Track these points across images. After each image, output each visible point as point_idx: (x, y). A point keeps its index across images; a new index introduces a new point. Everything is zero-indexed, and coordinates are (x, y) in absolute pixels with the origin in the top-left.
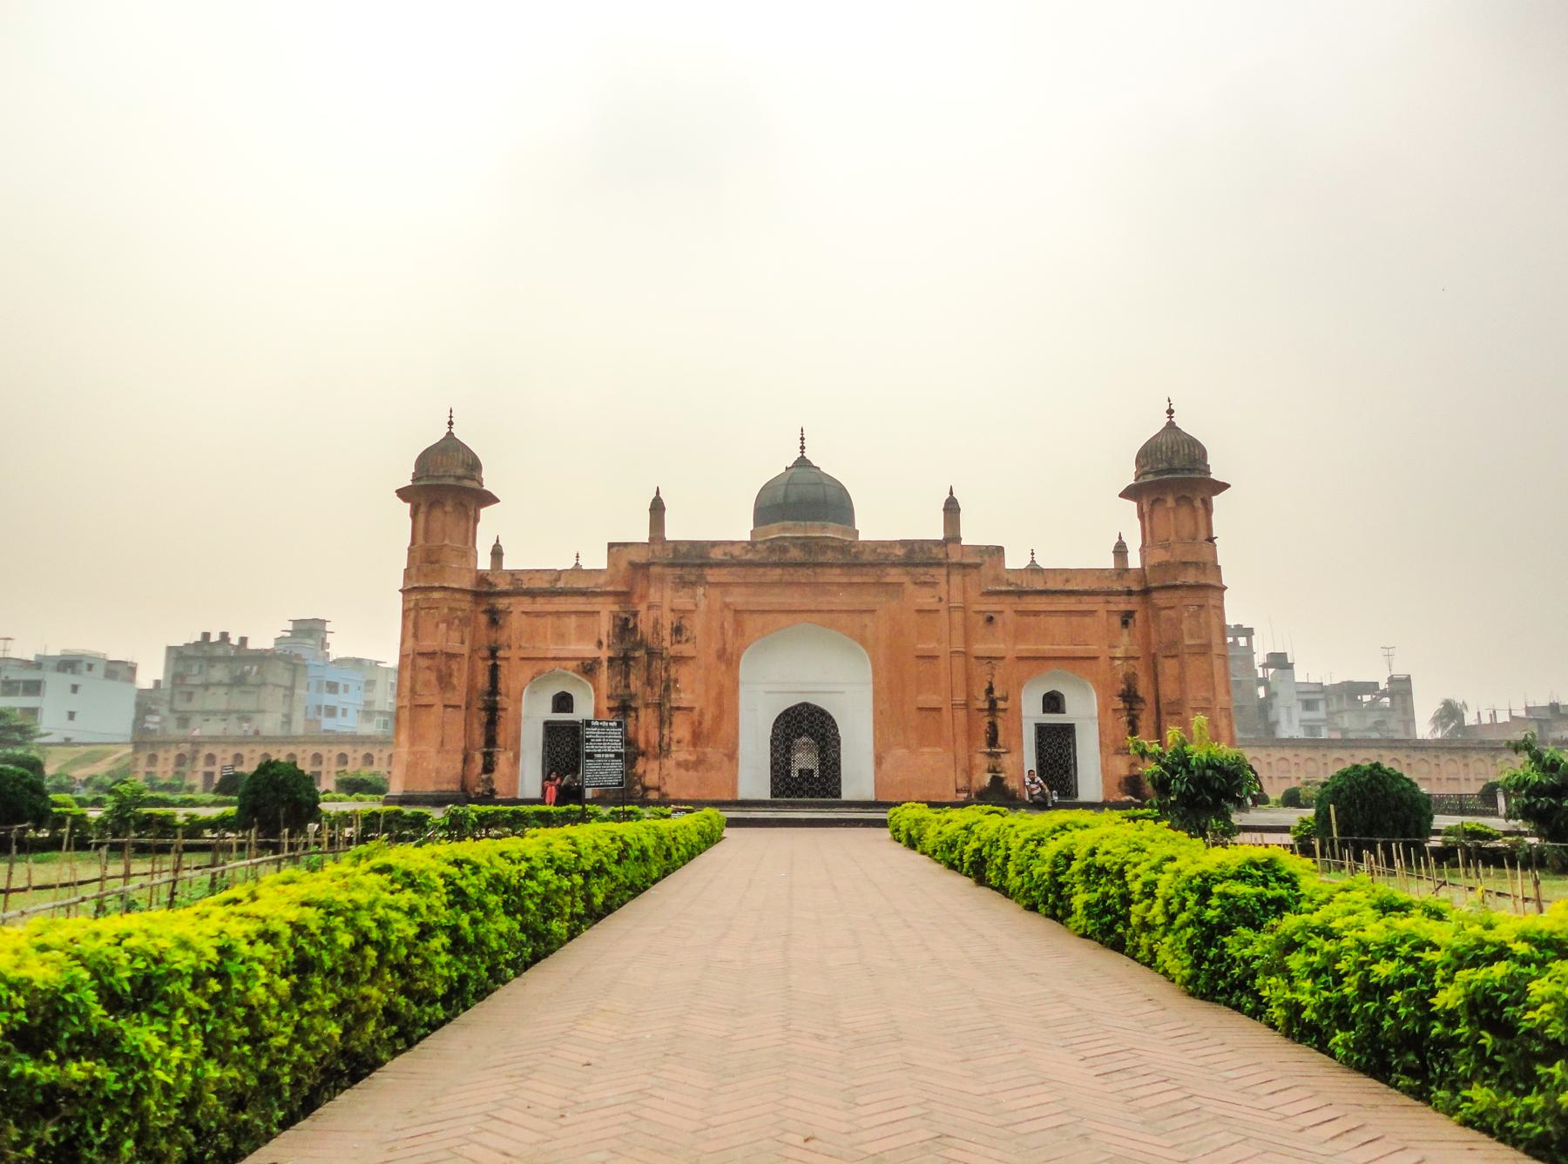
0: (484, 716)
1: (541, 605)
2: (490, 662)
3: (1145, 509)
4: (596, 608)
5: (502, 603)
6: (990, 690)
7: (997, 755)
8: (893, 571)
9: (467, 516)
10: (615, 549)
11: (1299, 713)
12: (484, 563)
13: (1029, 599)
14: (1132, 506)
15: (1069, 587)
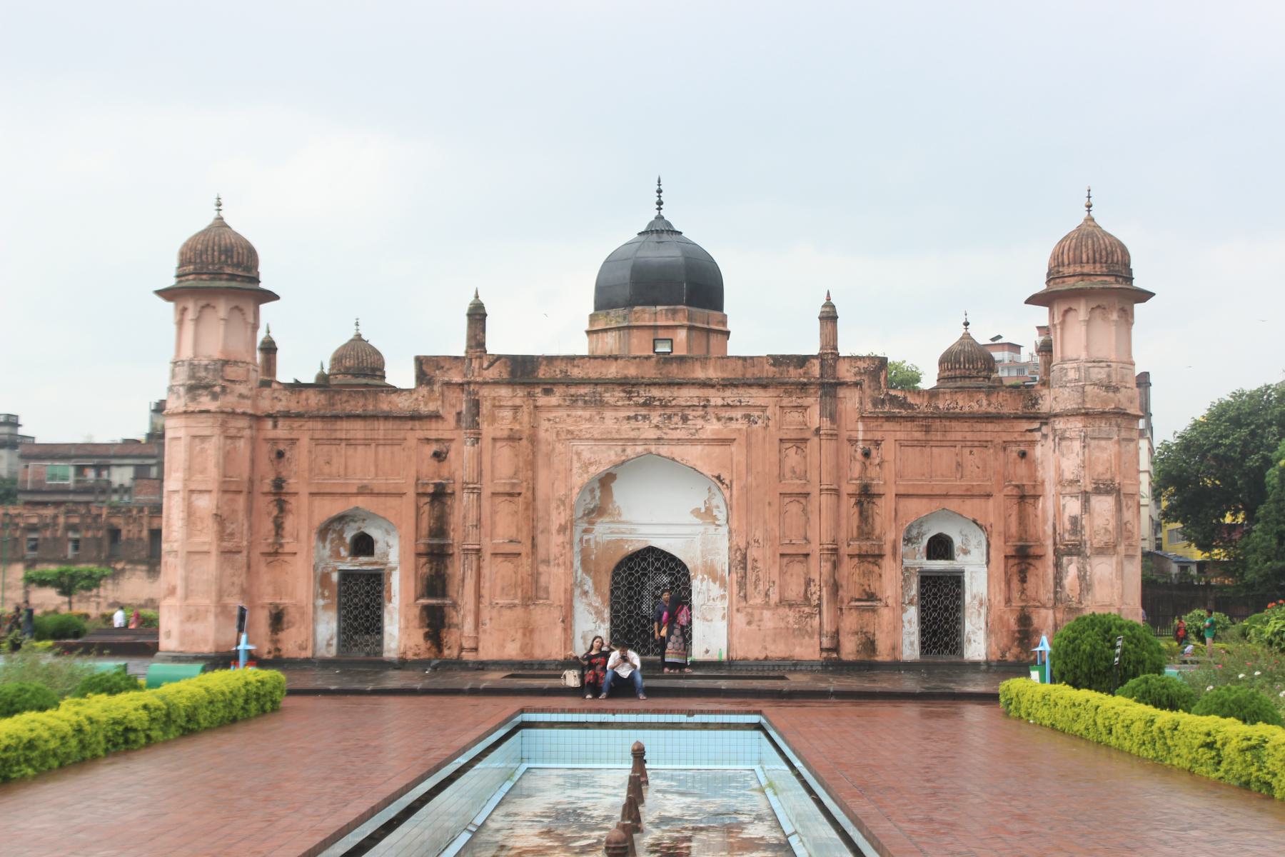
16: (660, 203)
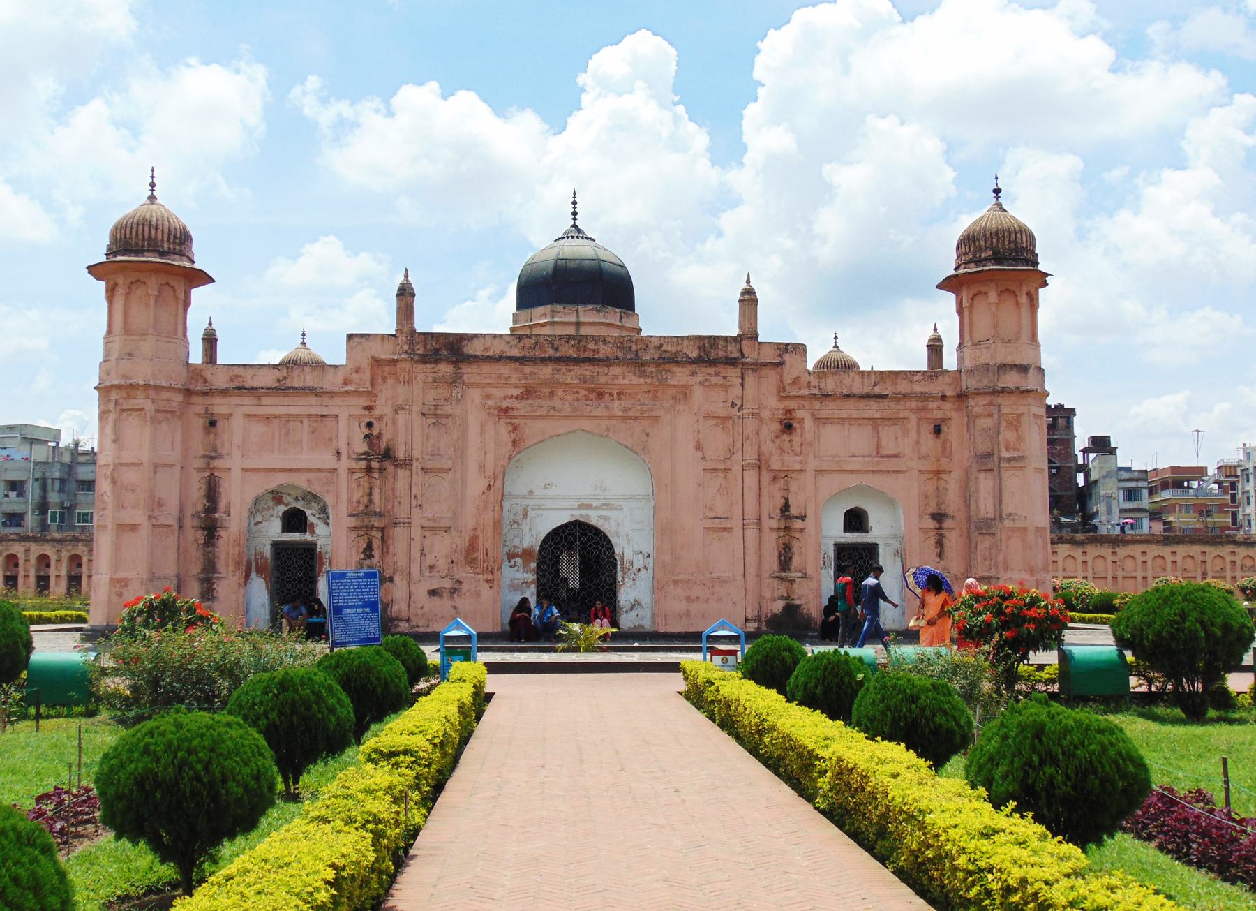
0: (201, 536)
1: (273, 406)
2: (207, 474)
3: (965, 304)
4: (334, 411)
5: (220, 406)
6: (786, 507)
7: (792, 582)
8: (678, 370)
9: (177, 299)
10: (356, 340)
11: (1121, 502)
12: (196, 356)
13: (831, 405)
14: (950, 299)
15: (877, 390)
16: (575, 213)
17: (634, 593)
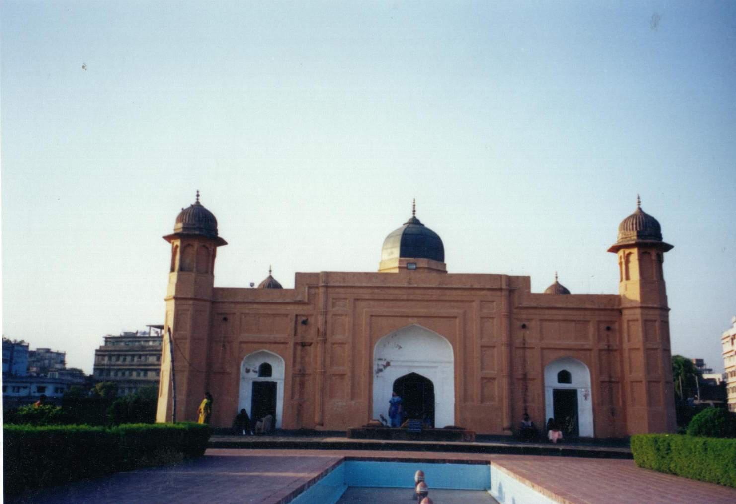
16: (414, 211)
17: (445, 414)
